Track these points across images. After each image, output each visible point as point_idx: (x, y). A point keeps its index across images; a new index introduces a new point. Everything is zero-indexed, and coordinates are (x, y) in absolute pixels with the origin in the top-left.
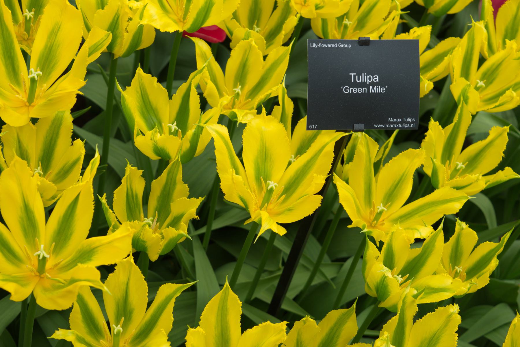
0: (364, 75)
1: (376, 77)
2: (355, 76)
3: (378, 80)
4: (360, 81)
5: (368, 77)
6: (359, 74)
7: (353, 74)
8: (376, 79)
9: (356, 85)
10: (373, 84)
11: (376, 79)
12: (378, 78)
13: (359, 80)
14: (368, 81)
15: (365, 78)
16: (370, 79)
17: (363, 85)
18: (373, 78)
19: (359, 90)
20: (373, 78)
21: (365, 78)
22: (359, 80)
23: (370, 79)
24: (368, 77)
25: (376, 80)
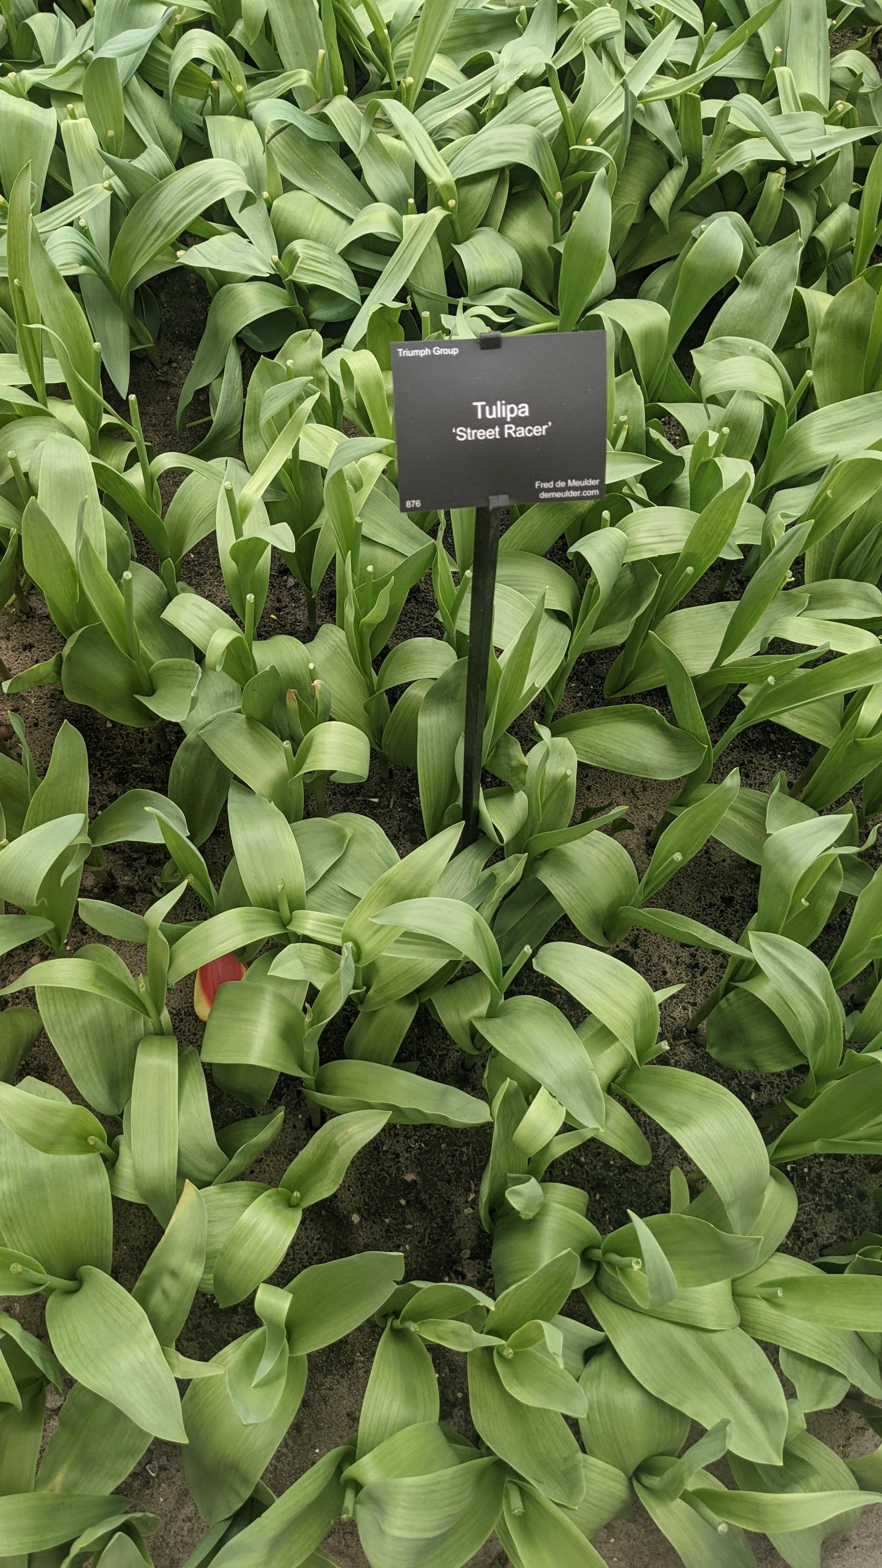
0: (502, 404)
1: (523, 407)
2: (483, 407)
3: (527, 414)
6: (491, 403)
7: (479, 404)
8: (524, 410)
9: (487, 424)
10: (518, 422)
11: (524, 410)
12: (527, 409)
13: (491, 413)
15: (501, 410)
16: (512, 411)
18: (519, 409)
20: (519, 409)
22: (491, 413)
23: (512, 411)
25: (523, 413)
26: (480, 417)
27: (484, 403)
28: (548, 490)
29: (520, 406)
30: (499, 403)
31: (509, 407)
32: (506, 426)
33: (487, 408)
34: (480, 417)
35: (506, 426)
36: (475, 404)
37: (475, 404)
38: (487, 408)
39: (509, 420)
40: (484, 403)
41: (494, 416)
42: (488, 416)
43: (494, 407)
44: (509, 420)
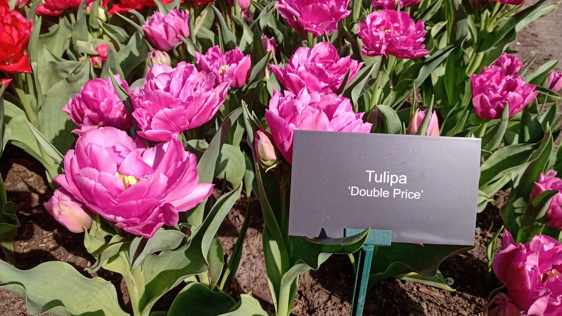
0: (387, 174)
1: (404, 178)
2: (373, 174)
3: (405, 182)
4: (381, 181)
7: (370, 172)
12: (405, 179)
13: (378, 179)
14: (392, 182)
15: (386, 178)
16: (394, 179)
17: (385, 186)
20: (399, 179)
21: (386, 178)
22: (378, 179)
23: (394, 179)
24: (392, 176)
26: (370, 181)
27: (374, 171)
29: (400, 177)
30: (385, 172)
31: (392, 176)
33: (376, 175)
34: (370, 181)
38: (376, 175)
39: (391, 185)
40: (374, 171)
41: (381, 181)
42: (376, 181)
43: (381, 175)
44: (391, 185)
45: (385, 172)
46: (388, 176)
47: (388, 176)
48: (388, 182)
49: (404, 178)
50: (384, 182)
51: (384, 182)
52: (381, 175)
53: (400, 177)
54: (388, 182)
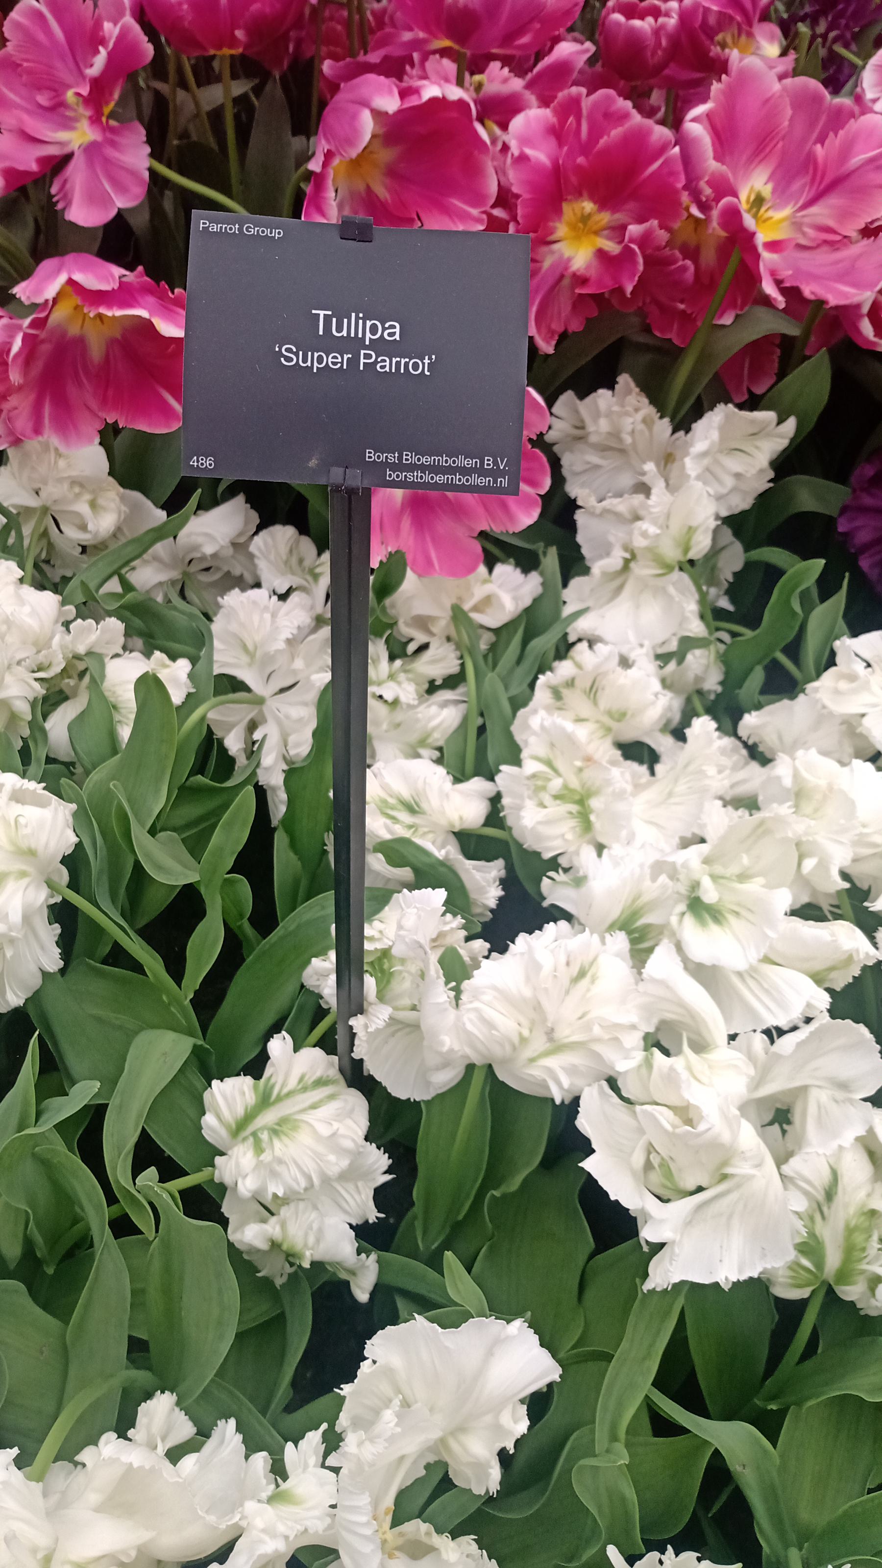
1: (394, 327)
2: (327, 319)
3: (397, 337)
5: (369, 323)
6: (341, 315)
7: (322, 313)
8: (394, 331)
10: (380, 346)
11: (394, 331)
12: (397, 330)
13: (339, 330)
17: (354, 344)
19: (335, 360)
20: (384, 329)
21: (354, 326)
22: (339, 330)
24: (369, 323)
25: (390, 335)
26: (321, 333)
27: (330, 313)
28: (398, 467)
29: (387, 325)
30: (353, 315)
31: (369, 323)
32: (362, 352)
33: (334, 320)
34: (321, 333)
35: (362, 352)
36: (314, 312)
37: (314, 312)
38: (334, 320)
39: (367, 343)
40: (330, 313)
43: (346, 320)
44: (367, 343)
45: (353, 315)
46: (361, 322)
47: (361, 322)
48: (360, 336)
49: (394, 327)
50: (353, 335)
51: (353, 335)
52: (346, 320)
53: (387, 325)
54: (360, 336)
